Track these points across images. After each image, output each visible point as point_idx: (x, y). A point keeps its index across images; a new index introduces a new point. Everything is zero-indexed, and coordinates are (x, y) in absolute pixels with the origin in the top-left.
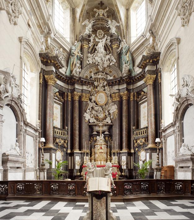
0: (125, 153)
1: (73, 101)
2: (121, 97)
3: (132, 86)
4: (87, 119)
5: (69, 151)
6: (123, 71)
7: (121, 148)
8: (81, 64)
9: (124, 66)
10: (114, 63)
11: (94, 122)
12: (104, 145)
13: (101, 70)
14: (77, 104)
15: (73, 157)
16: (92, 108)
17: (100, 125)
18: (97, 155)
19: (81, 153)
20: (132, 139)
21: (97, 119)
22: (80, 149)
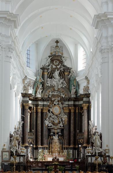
0: (72, 148)
1: (37, 112)
2: (70, 110)
3: (77, 102)
4: (47, 124)
5: (34, 146)
6: (71, 92)
7: (69, 144)
8: (43, 86)
9: (73, 88)
10: (65, 86)
11: (51, 126)
12: (58, 142)
13: (56, 90)
14: (39, 115)
15: (37, 150)
16: (50, 116)
17: (55, 128)
18: (53, 150)
19: (43, 148)
20: (77, 138)
21: (53, 123)
22: (42, 144)
